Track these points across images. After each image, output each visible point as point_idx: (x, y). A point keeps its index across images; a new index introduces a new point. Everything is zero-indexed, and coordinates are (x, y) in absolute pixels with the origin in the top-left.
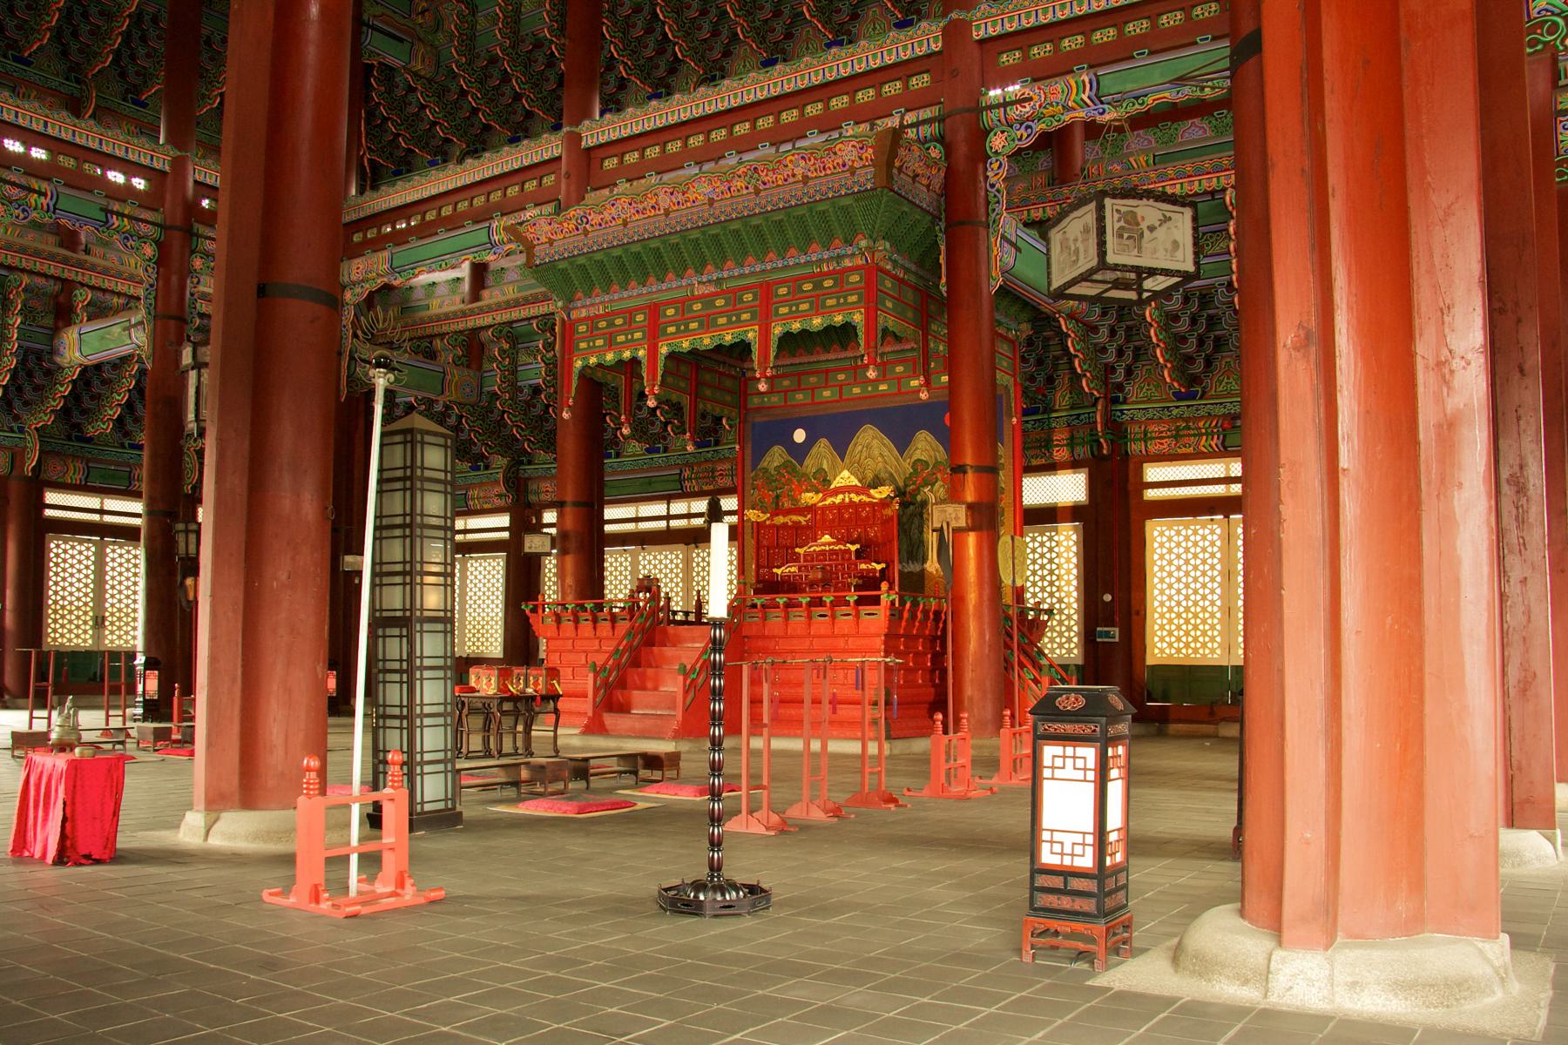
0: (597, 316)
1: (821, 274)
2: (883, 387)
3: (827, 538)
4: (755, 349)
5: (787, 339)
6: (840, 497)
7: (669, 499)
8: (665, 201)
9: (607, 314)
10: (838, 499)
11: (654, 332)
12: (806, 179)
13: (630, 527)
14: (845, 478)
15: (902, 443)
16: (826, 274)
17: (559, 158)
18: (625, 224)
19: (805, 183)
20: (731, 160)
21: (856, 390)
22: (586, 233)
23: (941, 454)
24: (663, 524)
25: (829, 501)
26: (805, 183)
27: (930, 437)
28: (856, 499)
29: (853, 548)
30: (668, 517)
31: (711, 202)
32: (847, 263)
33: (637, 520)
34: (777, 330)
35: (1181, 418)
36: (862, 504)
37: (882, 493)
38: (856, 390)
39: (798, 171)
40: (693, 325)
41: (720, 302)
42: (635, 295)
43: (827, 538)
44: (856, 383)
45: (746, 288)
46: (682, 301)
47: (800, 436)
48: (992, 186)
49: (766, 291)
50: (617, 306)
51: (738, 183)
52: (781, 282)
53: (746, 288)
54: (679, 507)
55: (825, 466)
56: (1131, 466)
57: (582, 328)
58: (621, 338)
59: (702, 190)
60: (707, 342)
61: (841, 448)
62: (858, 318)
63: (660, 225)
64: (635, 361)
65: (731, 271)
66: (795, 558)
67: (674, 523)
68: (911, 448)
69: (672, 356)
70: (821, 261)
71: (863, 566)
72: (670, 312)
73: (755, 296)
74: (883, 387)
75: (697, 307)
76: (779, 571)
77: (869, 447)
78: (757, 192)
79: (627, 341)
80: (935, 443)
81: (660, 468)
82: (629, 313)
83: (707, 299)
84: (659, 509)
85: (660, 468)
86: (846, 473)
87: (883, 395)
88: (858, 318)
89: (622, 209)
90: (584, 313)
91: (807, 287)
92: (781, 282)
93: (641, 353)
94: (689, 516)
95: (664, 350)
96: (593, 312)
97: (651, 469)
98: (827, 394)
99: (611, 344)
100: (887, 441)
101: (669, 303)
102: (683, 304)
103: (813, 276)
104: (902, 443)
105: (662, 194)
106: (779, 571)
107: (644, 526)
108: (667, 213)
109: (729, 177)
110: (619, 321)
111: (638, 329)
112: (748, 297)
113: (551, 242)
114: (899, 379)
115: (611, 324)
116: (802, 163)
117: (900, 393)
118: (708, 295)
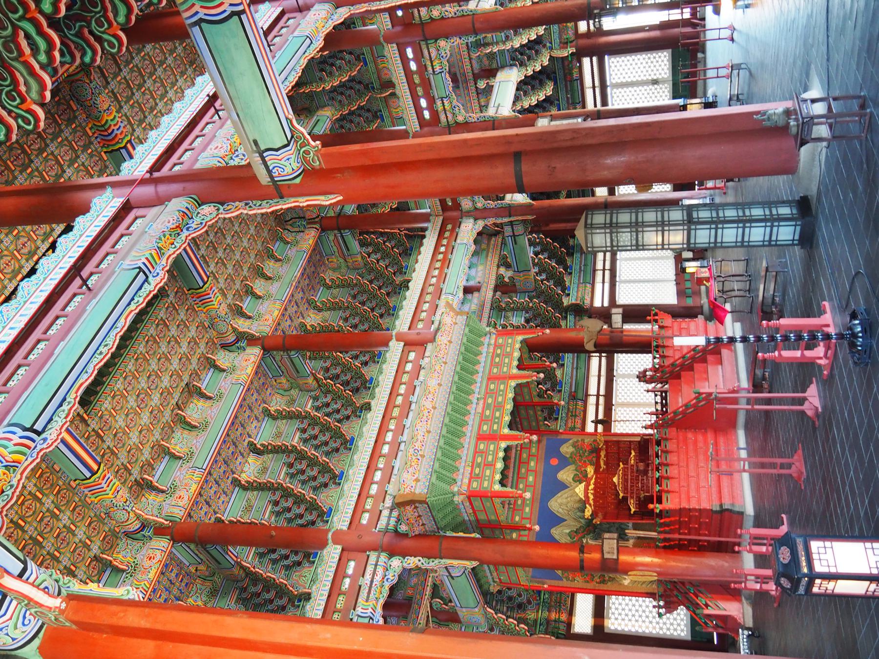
0: (471, 473)
3: (615, 480)
4: (520, 381)
5: (519, 367)
6: (590, 495)
8: (428, 405)
9: (472, 466)
10: (591, 497)
11: (492, 437)
12: (450, 342)
14: (580, 489)
17: (343, 550)
18: (429, 432)
20: (397, 464)
21: (527, 509)
22: (423, 456)
23: (572, 468)
25: (591, 502)
27: (562, 472)
28: (592, 487)
29: (622, 465)
32: (493, 342)
34: (515, 371)
35: (567, 414)
36: (595, 484)
37: (590, 470)
38: (527, 509)
39: (446, 342)
40: (497, 414)
41: (490, 401)
42: (468, 442)
43: (615, 480)
44: (523, 510)
46: (482, 420)
50: (470, 458)
55: (568, 531)
57: (475, 485)
58: (490, 458)
60: (509, 406)
61: (558, 520)
62: (520, 338)
64: (507, 450)
65: (476, 388)
66: (625, 499)
68: (566, 482)
69: (510, 427)
71: (632, 462)
72: (485, 428)
75: (488, 413)
76: (633, 510)
77: (561, 505)
78: (445, 363)
79: (493, 455)
86: (577, 490)
88: (520, 338)
89: (421, 428)
90: (466, 481)
91: (497, 360)
93: (503, 445)
95: (506, 431)
99: (492, 465)
100: (559, 495)
103: (492, 357)
104: (563, 486)
105: (425, 403)
106: (633, 510)
110: (479, 460)
111: (487, 447)
113: (417, 480)
115: (479, 465)
117: (535, 471)
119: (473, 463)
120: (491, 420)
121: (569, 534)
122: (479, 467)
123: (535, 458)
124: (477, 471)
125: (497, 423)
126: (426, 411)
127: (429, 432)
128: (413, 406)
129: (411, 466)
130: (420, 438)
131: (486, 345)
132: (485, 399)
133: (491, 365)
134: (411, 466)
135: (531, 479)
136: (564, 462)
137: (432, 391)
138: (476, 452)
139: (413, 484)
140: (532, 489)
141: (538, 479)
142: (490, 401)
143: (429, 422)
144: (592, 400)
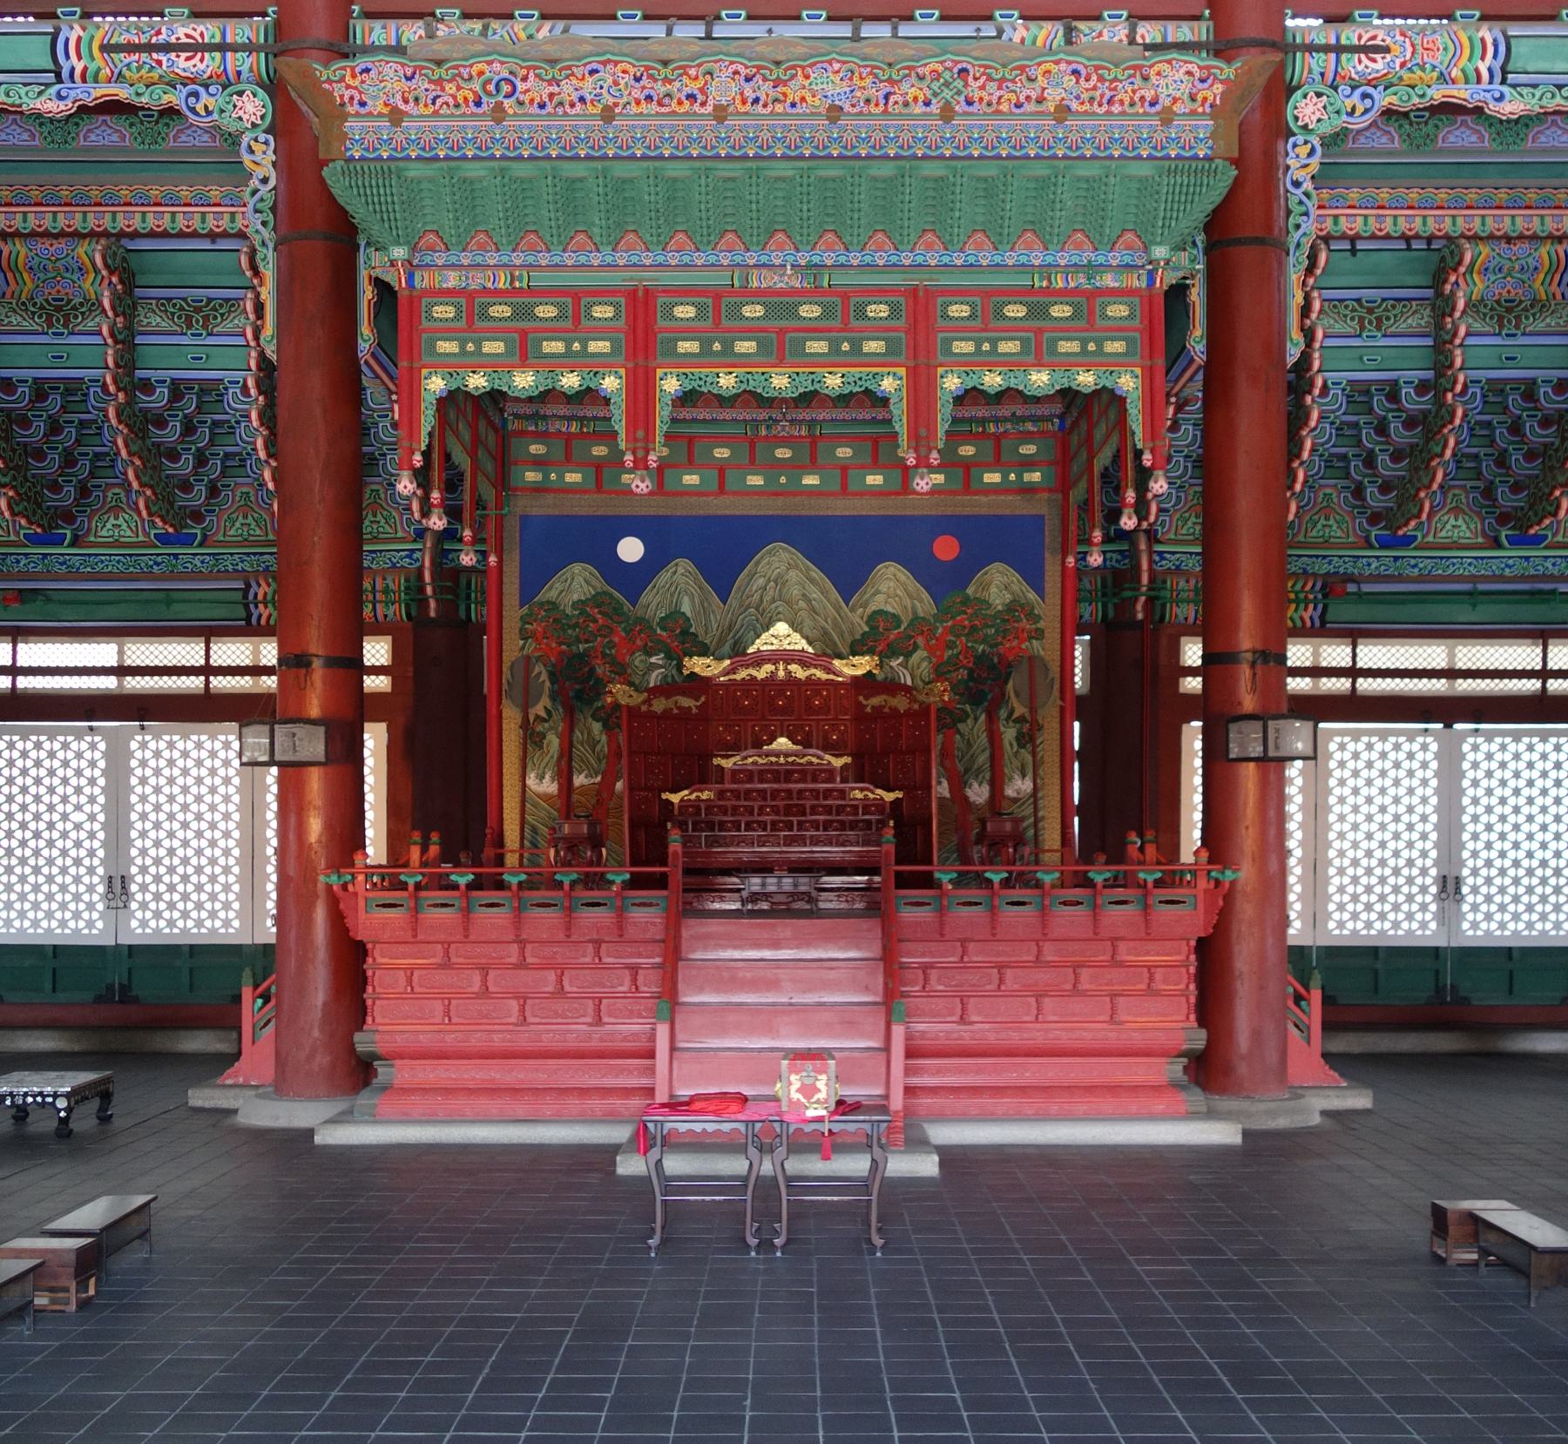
0: (485, 291)
1: (1048, 291)
2: (811, 480)
7: (208, 633)
8: (723, 89)
9: (514, 292)
12: (1063, 111)
13: (109, 683)
15: (849, 582)
16: (1064, 293)
18: (608, 115)
19: (1060, 121)
21: (755, 480)
22: (498, 113)
24: (194, 683)
26: (1060, 121)
30: (207, 670)
31: (835, 112)
32: (1108, 281)
33: (121, 671)
38: (755, 480)
39: (1054, 95)
41: (810, 311)
44: (753, 464)
45: (879, 292)
46: (717, 295)
47: (631, 549)
48: (1297, 184)
49: (919, 310)
50: (541, 280)
51: (910, 89)
52: (959, 293)
53: (879, 292)
54: (230, 652)
56: (1164, 641)
59: (828, 85)
63: (698, 131)
67: (220, 683)
70: (1047, 269)
72: (685, 312)
73: (894, 311)
74: (811, 480)
75: (753, 311)
78: (947, 113)
80: (913, 585)
81: (197, 575)
82: (576, 301)
83: (781, 302)
84: (188, 652)
85: (197, 575)
87: (812, 492)
90: (452, 280)
92: (959, 293)
94: (256, 671)
96: (478, 281)
97: (172, 576)
98: (691, 479)
100: (816, 573)
101: (685, 293)
102: (718, 303)
105: (724, 75)
107: (135, 684)
108: (720, 113)
109: (890, 70)
110: (546, 311)
111: (600, 332)
112: (878, 310)
114: (844, 470)
116: (1069, 81)
118: (793, 292)
119: (531, 291)
120: (988, 319)
121: (674, 618)
122: (516, 315)
123: (959, 486)
124: (501, 311)
125: (835, 348)
126: (694, 87)
127: (608, 115)
128: (689, 31)
129: (439, 82)
130: (567, 90)
131: (1087, 256)
132: (815, 293)
133: (987, 293)
134: (439, 82)
135: (874, 480)
136: (948, 582)
137: (793, 91)
138: (576, 295)
139: (378, 106)
140: (837, 487)
141: (875, 502)
142: (810, 311)
143: (644, 108)
144: (1432, 654)
